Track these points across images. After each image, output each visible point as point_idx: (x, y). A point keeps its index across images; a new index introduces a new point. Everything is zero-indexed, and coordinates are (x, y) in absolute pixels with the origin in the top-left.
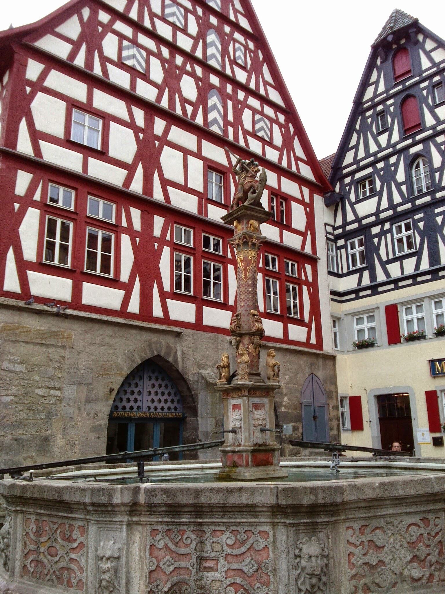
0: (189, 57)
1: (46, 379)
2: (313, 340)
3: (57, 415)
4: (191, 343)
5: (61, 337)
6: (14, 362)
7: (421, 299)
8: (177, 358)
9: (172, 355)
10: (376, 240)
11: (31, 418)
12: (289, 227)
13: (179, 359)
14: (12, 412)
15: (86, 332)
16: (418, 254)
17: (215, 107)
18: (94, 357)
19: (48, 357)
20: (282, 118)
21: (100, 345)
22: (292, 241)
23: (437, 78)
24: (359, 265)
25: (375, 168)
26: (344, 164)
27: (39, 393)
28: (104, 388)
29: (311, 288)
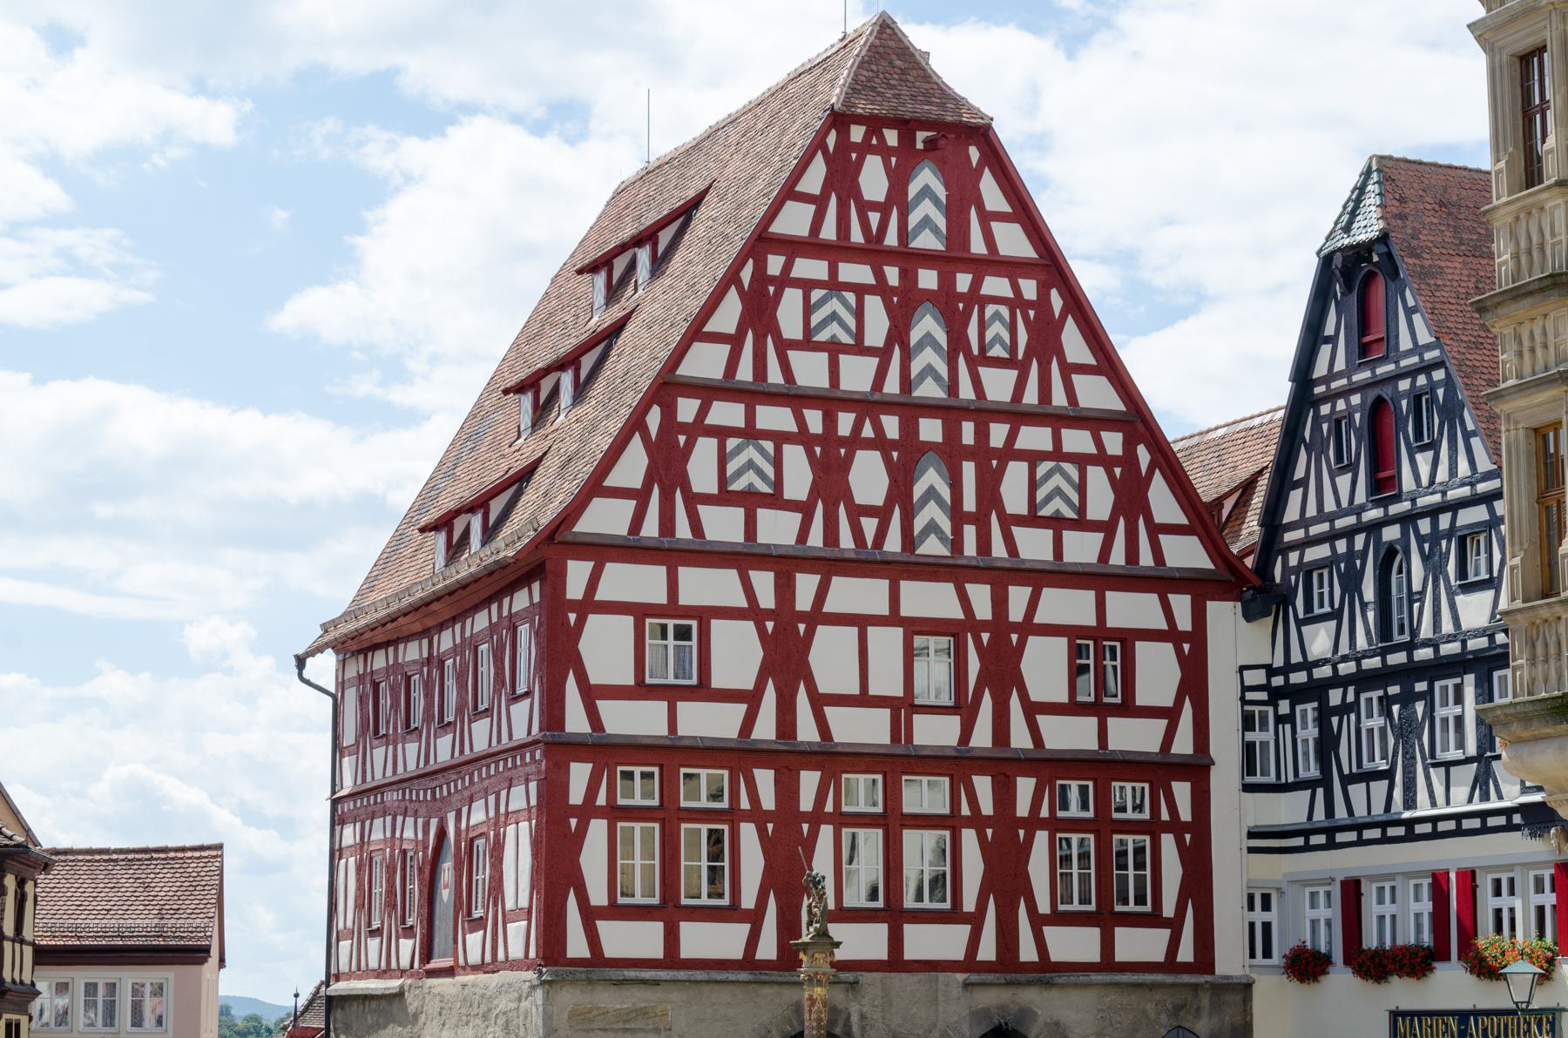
0: (868, 406)
2: (1186, 953)
7: (1391, 877)
9: (841, 1022)
10: (1335, 720)
12: (1128, 708)
13: (855, 1029)
16: (1388, 775)
17: (931, 493)
20: (1114, 442)
22: (1135, 736)
23: (1422, 380)
24: (1314, 772)
25: (1333, 549)
26: (1286, 520)
29: (1188, 837)
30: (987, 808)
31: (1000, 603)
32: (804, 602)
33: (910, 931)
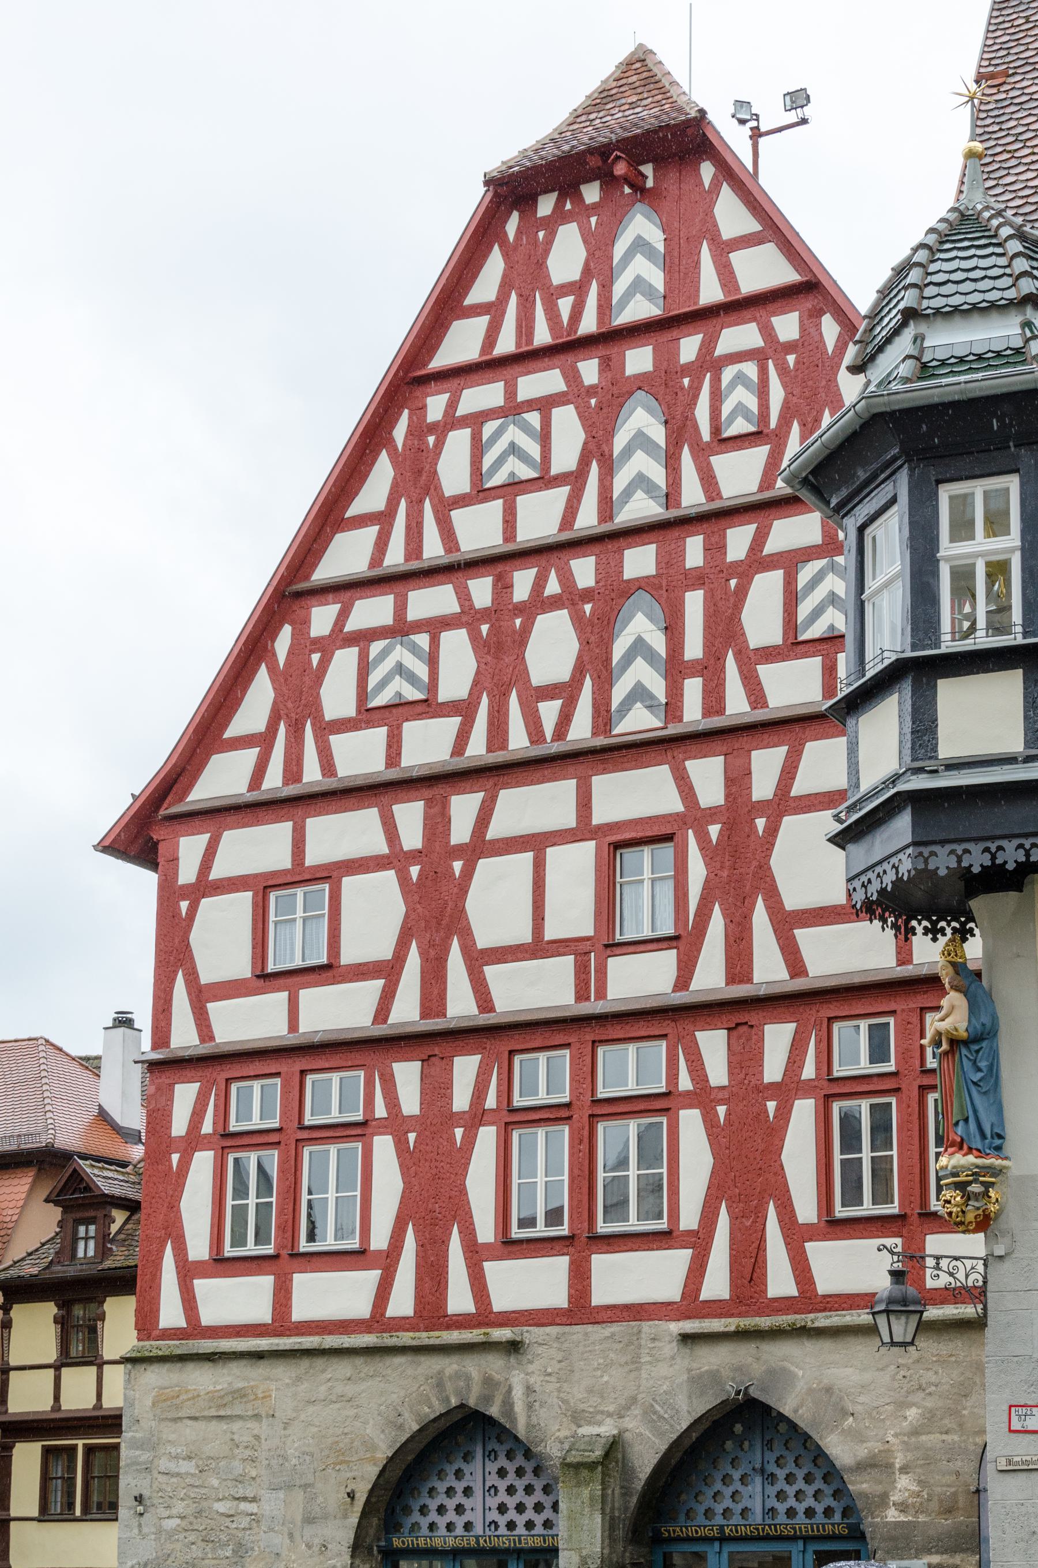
1: (229, 1483)
3: (252, 1549)
4: (555, 1362)
5: (252, 1397)
6: (176, 1457)
8: (511, 1405)
9: (498, 1400)
11: (210, 1556)
13: (519, 1407)
14: (178, 1546)
15: (299, 1379)
17: (639, 647)
18: (315, 1430)
19: (232, 1440)
21: (326, 1401)
27: (221, 1510)
28: (338, 1492)
30: (718, 1073)
31: (737, 781)
32: (461, 832)
33: (600, 1262)
